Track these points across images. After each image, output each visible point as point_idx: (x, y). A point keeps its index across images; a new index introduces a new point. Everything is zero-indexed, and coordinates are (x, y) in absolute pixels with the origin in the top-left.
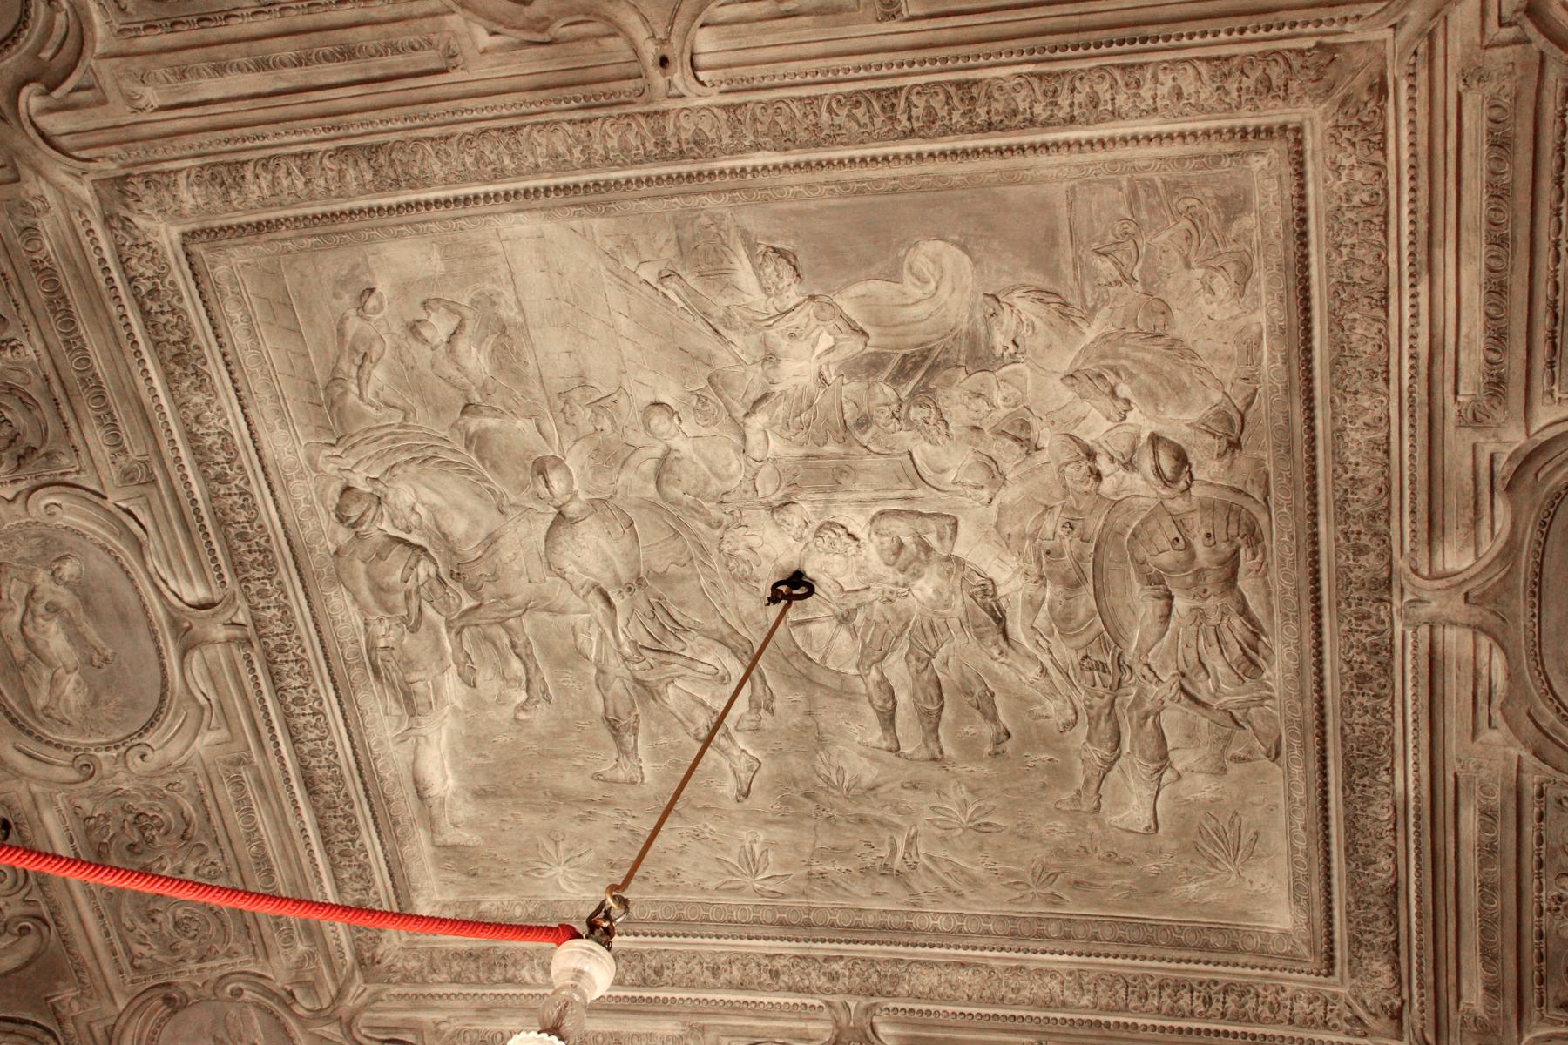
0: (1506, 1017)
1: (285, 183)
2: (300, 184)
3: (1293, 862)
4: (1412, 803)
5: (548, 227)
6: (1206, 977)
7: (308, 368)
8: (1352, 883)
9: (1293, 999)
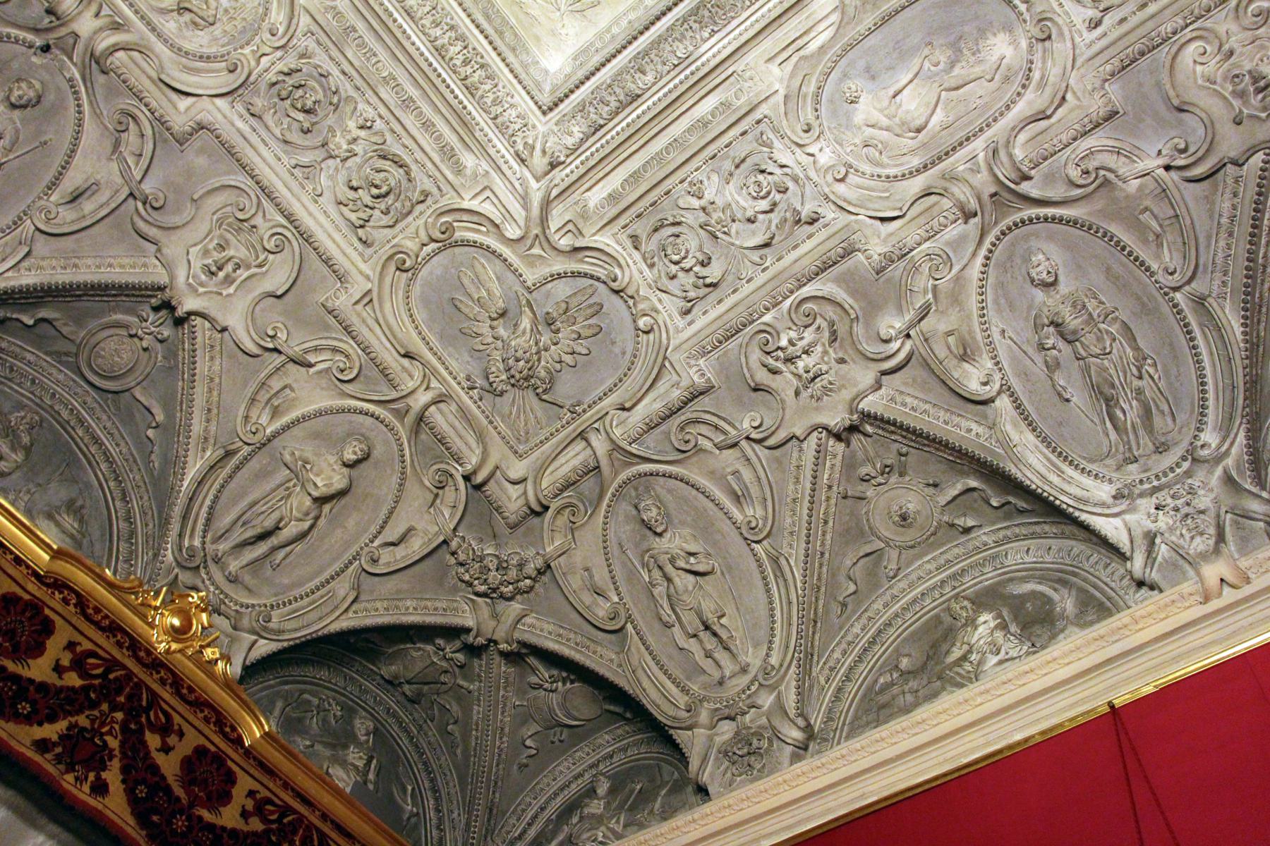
0: (601, 218)
3: (599, 37)
4: (699, 63)
6: (480, 50)
8: (620, 73)
9: (512, 106)
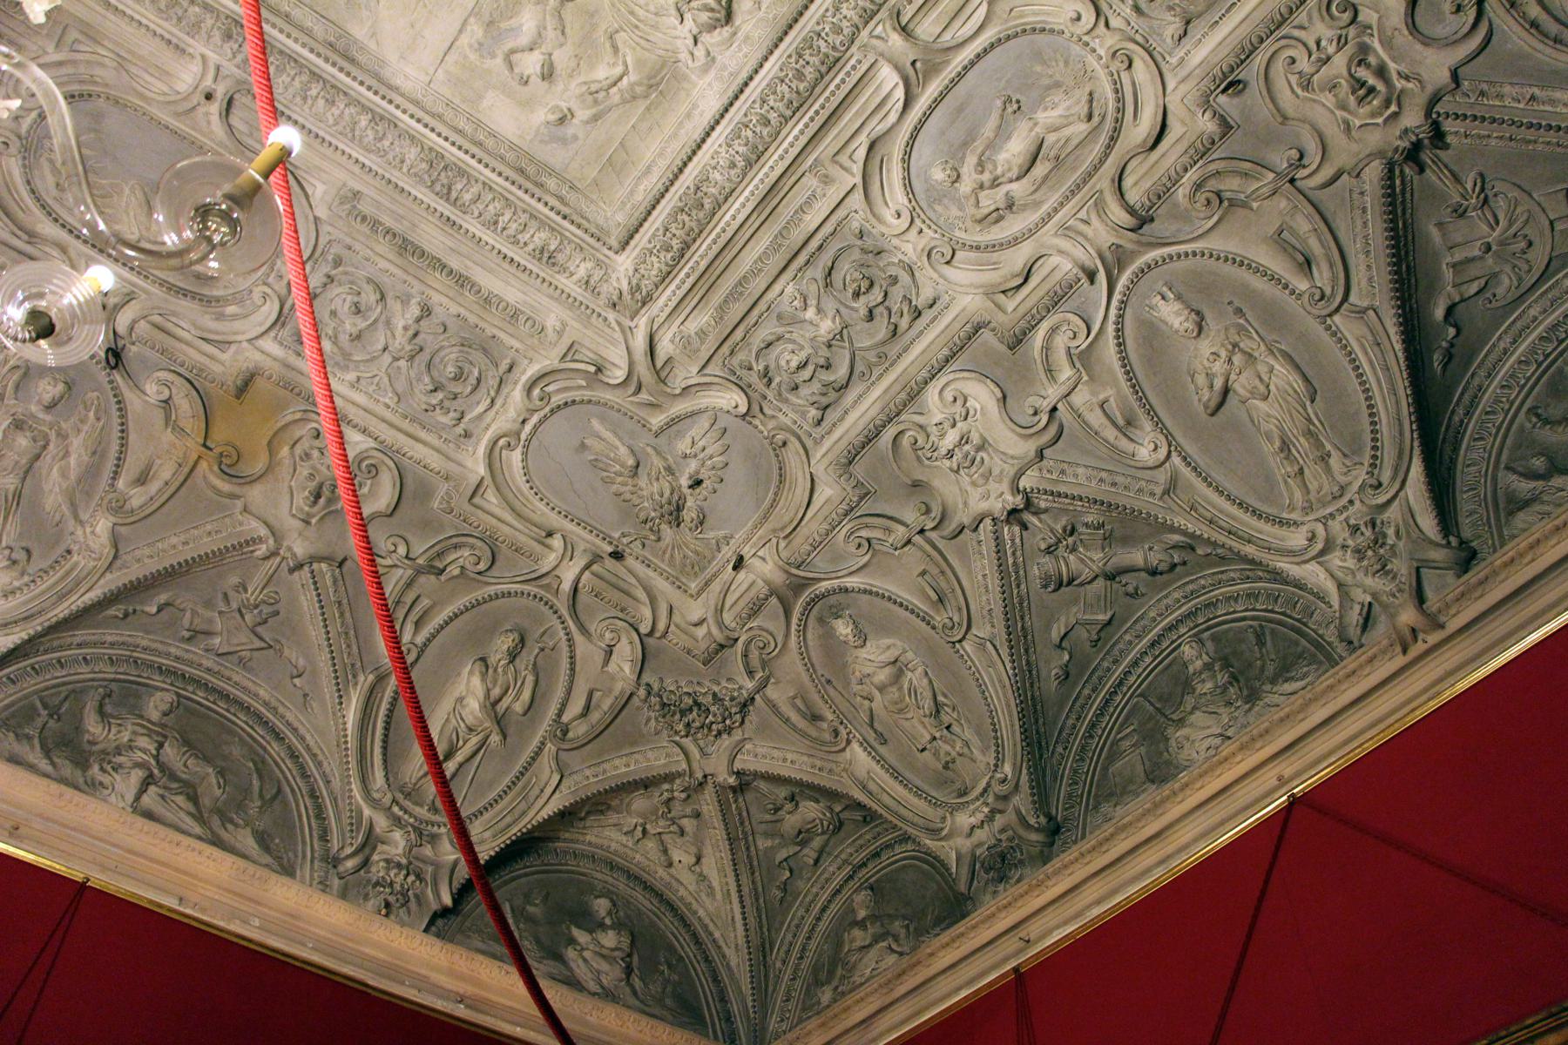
1: (514, 226)
2: (507, 217)
5: (392, 56)
7: (642, 119)
